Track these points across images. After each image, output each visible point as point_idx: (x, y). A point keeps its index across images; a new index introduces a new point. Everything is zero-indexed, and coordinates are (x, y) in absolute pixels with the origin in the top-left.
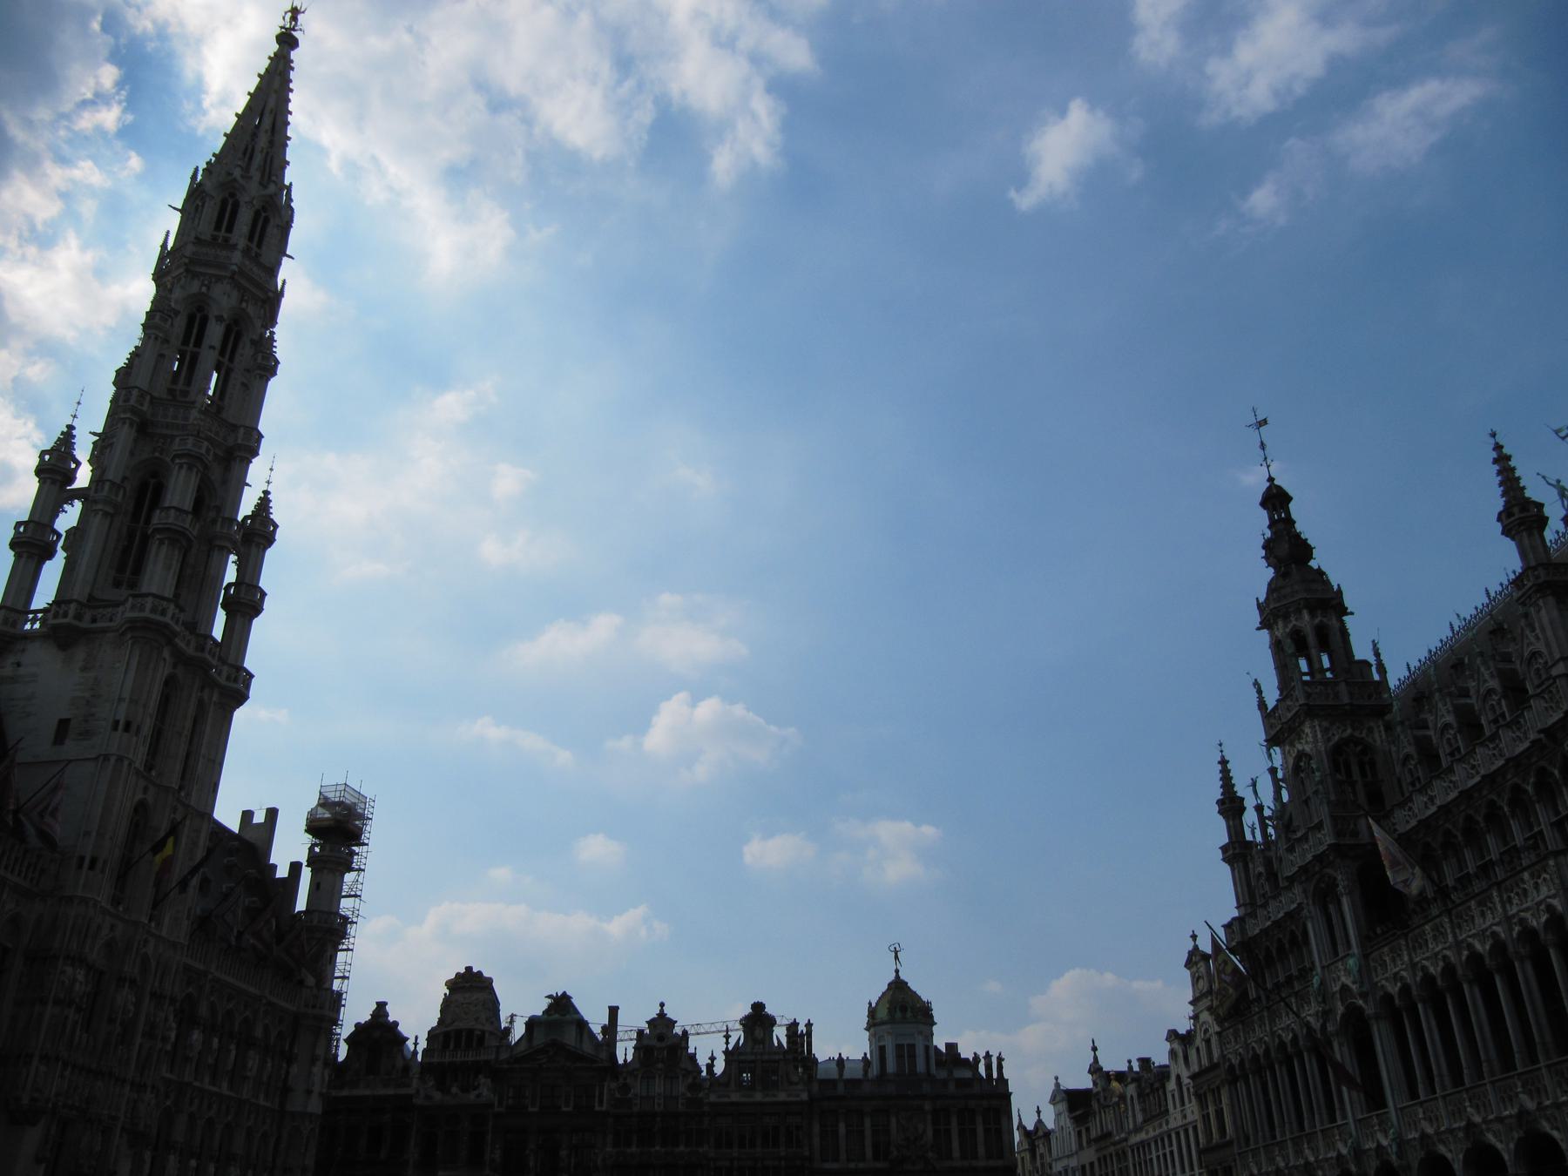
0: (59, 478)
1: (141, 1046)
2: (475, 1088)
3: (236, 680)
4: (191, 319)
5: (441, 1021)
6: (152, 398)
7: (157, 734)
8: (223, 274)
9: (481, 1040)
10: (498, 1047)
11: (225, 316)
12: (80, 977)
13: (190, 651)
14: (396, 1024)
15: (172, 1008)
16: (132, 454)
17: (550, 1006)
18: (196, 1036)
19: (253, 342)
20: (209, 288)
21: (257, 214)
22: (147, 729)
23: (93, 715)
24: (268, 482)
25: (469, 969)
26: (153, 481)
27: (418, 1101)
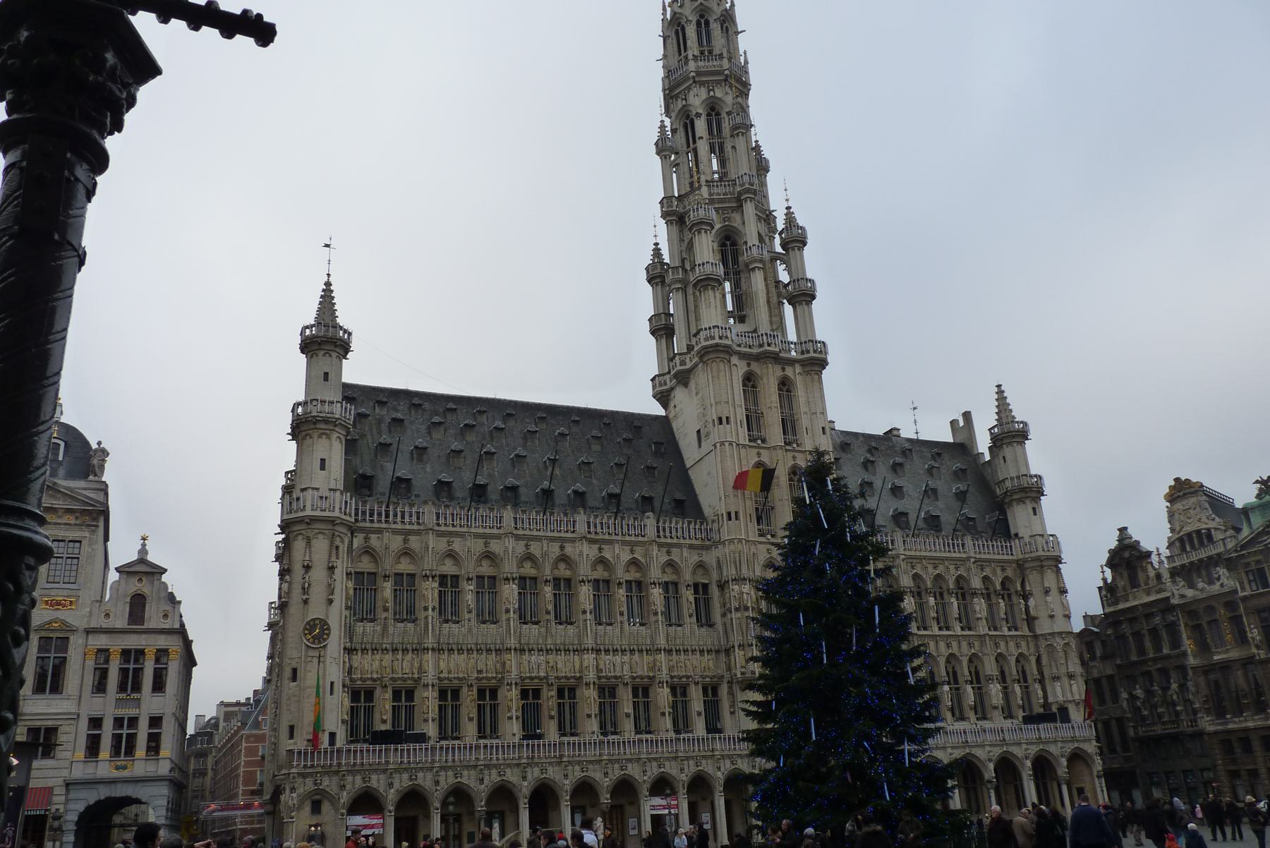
2: (1218, 579)
3: (808, 352)
5: (1172, 530)
10: (1223, 540)
11: (700, 111)
12: (747, 588)
13: (755, 350)
14: (1138, 542)
16: (682, 240)
17: (1260, 489)
19: (729, 113)
21: (698, 24)
22: (741, 414)
24: (787, 200)
25: (1177, 480)
27: (1175, 601)
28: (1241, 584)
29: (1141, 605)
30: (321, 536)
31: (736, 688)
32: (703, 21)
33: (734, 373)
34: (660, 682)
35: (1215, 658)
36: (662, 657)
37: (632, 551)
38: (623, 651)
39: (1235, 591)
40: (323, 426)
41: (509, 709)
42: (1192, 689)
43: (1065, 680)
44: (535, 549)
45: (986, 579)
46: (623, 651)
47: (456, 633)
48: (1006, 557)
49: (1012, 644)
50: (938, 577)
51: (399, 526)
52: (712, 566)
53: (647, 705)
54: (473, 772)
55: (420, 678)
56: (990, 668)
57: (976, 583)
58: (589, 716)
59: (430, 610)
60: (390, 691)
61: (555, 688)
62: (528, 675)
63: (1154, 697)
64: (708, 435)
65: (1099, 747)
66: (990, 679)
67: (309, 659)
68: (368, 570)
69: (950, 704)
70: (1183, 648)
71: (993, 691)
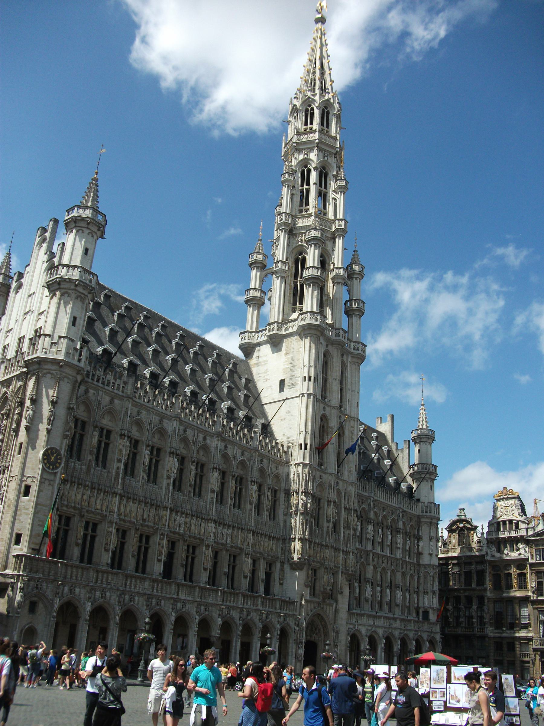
0: (259, 265)
1: (344, 533)
2: (518, 550)
3: (358, 349)
4: (303, 172)
6: (293, 216)
7: (325, 381)
8: (313, 146)
9: (517, 527)
10: (527, 529)
11: (318, 167)
13: (334, 338)
15: (355, 515)
18: (370, 528)
20: (308, 155)
22: (320, 380)
23: (294, 375)
26: (300, 257)
27: (488, 558)
28: (532, 555)
29: (464, 556)
30: (66, 379)
31: (287, 567)
32: (326, 111)
33: (320, 349)
34: (248, 554)
35: (504, 595)
36: (251, 535)
37: (243, 454)
38: (229, 526)
39: (528, 559)
40: (80, 289)
41: (160, 555)
42: (486, 610)
43: (431, 594)
44: (190, 433)
45: (404, 523)
46: (229, 526)
47: (134, 485)
48: (413, 512)
49: (408, 568)
50: (385, 516)
51: (110, 389)
52: (283, 479)
53: (234, 567)
54: (141, 599)
55: (106, 516)
56: (399, 579)
57: (401, 525)
58: (205, 569)
59: (123, 462)
60: (84, 519)
61: (187, 543)
62: (173, 530)
63: (460, 611)
64: (293, 385)
65: (441, 638)
66: (397, 587)
67: (43, 480)
68: (82, 418)
69: (379, 599)
70: (485, 586)
71: (399, 595)
